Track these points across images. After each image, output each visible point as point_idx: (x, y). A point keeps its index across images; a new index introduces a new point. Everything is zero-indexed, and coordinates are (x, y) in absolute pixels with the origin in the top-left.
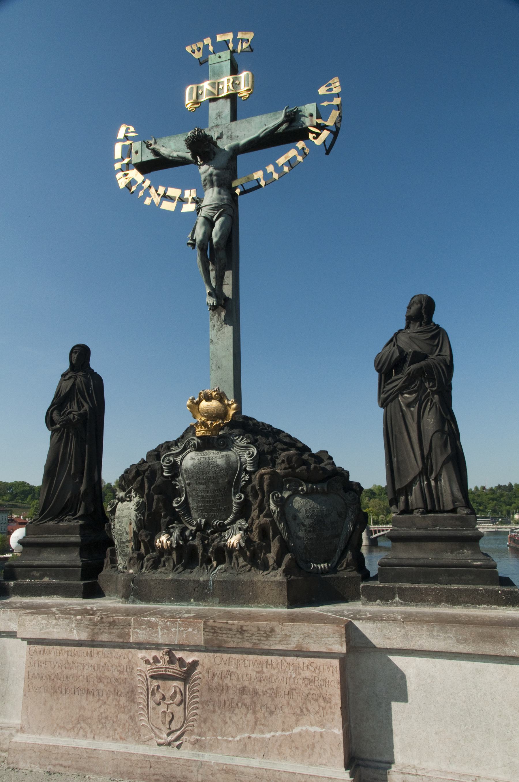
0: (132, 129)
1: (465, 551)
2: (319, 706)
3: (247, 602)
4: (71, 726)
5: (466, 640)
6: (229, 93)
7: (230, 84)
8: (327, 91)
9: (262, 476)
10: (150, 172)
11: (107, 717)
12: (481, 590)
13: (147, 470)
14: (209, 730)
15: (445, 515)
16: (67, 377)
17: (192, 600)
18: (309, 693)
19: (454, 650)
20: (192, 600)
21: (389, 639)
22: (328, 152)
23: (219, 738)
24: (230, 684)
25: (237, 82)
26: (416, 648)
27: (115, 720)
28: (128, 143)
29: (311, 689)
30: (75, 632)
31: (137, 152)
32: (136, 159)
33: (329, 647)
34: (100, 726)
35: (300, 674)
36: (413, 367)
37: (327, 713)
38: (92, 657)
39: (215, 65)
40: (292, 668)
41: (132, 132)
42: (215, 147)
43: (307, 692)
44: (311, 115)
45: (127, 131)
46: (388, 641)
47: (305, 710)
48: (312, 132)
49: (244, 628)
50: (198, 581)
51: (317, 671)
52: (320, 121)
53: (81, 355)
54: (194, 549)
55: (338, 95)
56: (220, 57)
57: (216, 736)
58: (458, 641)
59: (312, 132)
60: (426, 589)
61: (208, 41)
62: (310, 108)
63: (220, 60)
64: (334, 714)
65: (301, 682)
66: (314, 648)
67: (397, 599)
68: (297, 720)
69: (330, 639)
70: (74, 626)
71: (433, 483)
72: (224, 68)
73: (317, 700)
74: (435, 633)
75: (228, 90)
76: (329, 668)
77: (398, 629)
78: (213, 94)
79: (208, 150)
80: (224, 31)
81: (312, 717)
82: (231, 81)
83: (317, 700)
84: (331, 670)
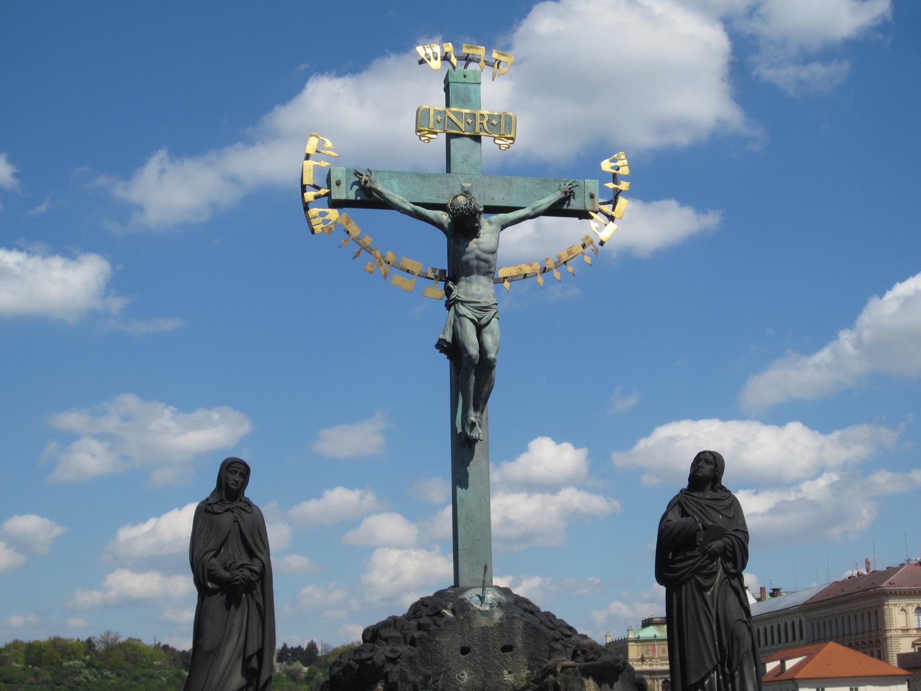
0: (329, 144)
7: (485, 122)
8: (612, 168)
9: (564, 668)
13: (399, 657)
25: (494, 122)
31: (338, 184)
32: (340, 194)
36: (716, 544)
39: (459, 85)
41: (330, 149)
44: (592, 196)
45: (322, 143)
55: (625, 178)
56: (465, 76)
61: (449, 47)
62: (592, 185)
63: (466, 80)
72: (472, 94)
82: (487, 118)
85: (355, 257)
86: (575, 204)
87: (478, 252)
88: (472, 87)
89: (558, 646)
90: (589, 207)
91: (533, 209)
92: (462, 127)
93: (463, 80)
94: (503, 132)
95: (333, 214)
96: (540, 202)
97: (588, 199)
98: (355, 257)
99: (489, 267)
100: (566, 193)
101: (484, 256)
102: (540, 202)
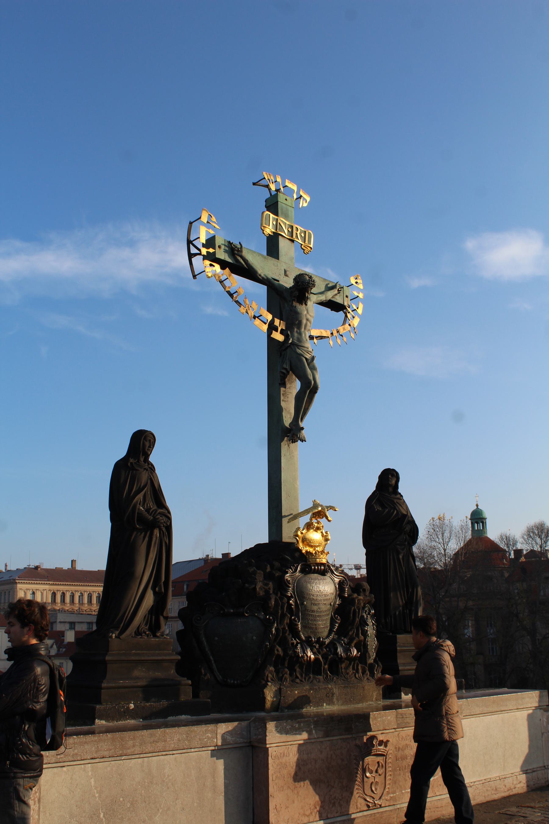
4: (309, 812)
11: (335, 798)
14: (398, 788)
17: (325, 704)
20: (325, 704)
23: (403, 791)
24: (407, 753)
27: (341, 798)
28: (212, 232)
30: (314, 732)
32: (221, 255)
34: (331, 806)
38: (321, 752)
56: (286, 200)
57: (401, 791)
70: (312, 727)
80: (292, 181)
95: (217, 267)
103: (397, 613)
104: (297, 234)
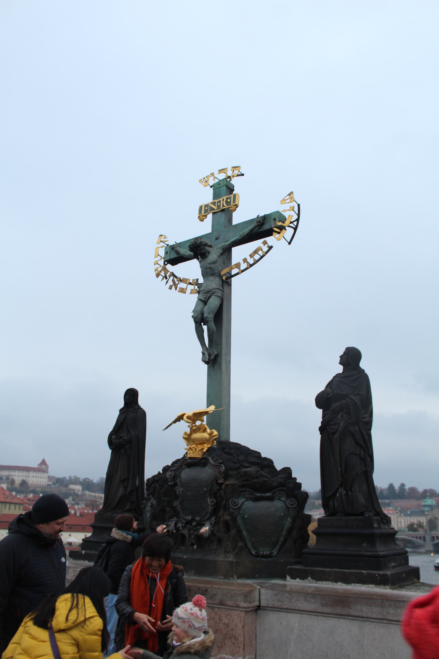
1: (364, 544)
2: (232, 642)
3: (211, 574)
5: (326, 605)
6: (224, 208)
10: (177, 264)
12: (365, 573)
15: (353, 518)
16: (122, 411)
18: (226, 634)
19: (319, 610)
21: (281, 601)
22: (290, 243)
25: (229, 200)
26: (296, 608)
29: (227, 631)
33: (238, 603)
35: (222, 620)
37: (236, 647)
40: (218, 617)
42: (209, 248)
43: (225, 633)
44: (275, 219)
46: (280, 603)
47: (223, 644)
48: (275, 232)
49: (191, 588)
50: (183, 558)
51: (231, 619)
52: (280, 224)
53: (131, 396)
54: (183, 536)
58: (323, 605)
59: (275, 232)
60: (329, 571)
63: (220, 186)
64: (239, 648)
65: (222, 626)
66: (230, 603)
67: (309, 578)
68: (219, 650)
69: (238, 598)
71: (350, 493)
73: (230, 638)
74: (308, 599)
75: (223, 206)
76: (238, 618)
77: (286, 595)
78: (214, 209)
79: (203, 251)
81: (227, 648)
83: (230, 638)
84: (239, 619)
85: (166, 284)
86: (266, 227)
87: (206, 265)
88: (222, 188)
89: (234, 473)
90: (273, 226)
91: (240, 235)
92: (215, 208)
93: (218, 186)
94: (232, 203)
96: (244, 231)
97: (272, 222)
98: (166, 284)
99: (213, 271)
100: (259, 222)
101: (209, 266)
102: (244, 231)
103: (338, 495)
104: (223, 203)
